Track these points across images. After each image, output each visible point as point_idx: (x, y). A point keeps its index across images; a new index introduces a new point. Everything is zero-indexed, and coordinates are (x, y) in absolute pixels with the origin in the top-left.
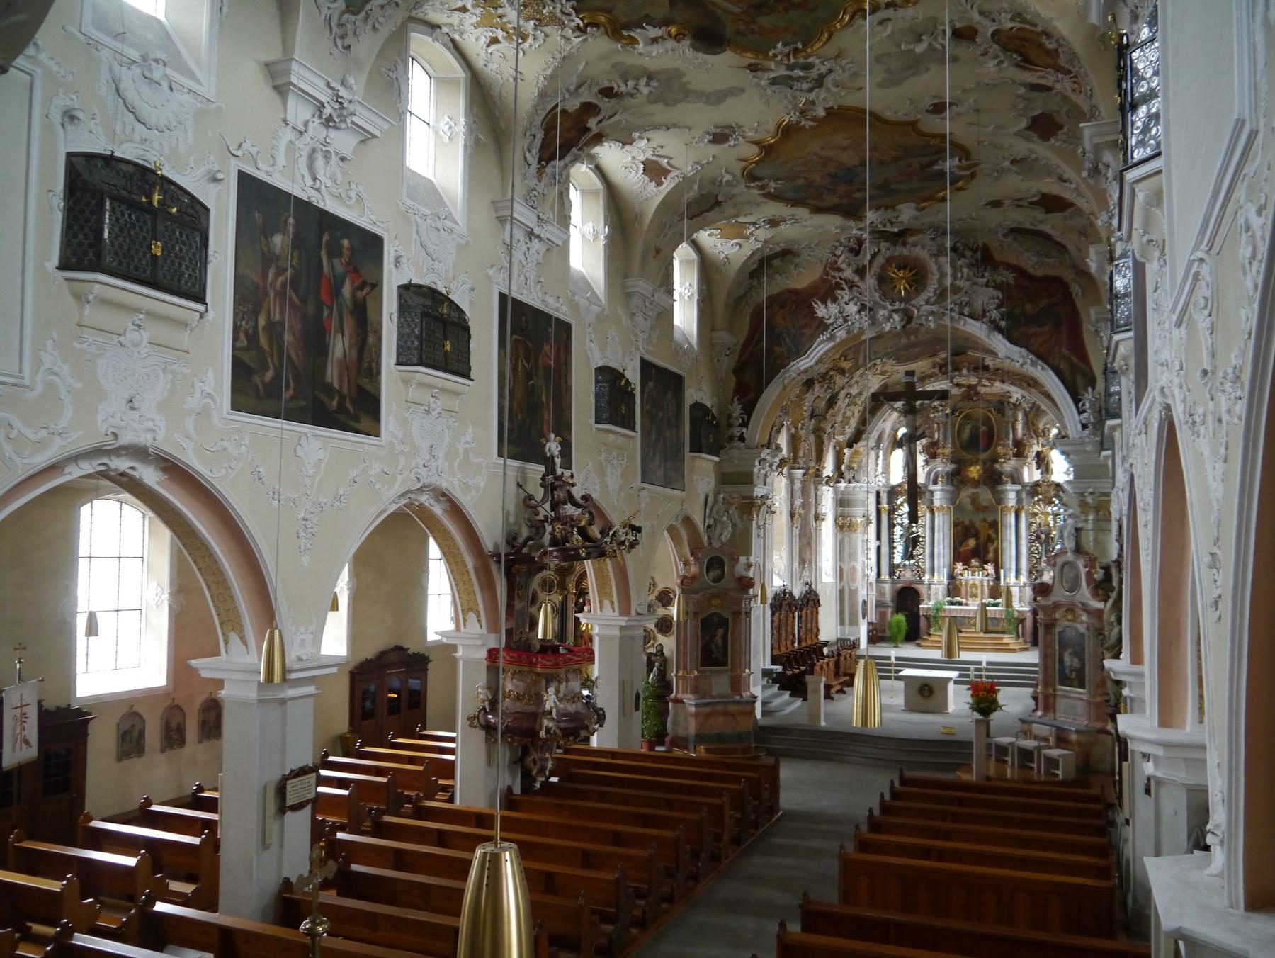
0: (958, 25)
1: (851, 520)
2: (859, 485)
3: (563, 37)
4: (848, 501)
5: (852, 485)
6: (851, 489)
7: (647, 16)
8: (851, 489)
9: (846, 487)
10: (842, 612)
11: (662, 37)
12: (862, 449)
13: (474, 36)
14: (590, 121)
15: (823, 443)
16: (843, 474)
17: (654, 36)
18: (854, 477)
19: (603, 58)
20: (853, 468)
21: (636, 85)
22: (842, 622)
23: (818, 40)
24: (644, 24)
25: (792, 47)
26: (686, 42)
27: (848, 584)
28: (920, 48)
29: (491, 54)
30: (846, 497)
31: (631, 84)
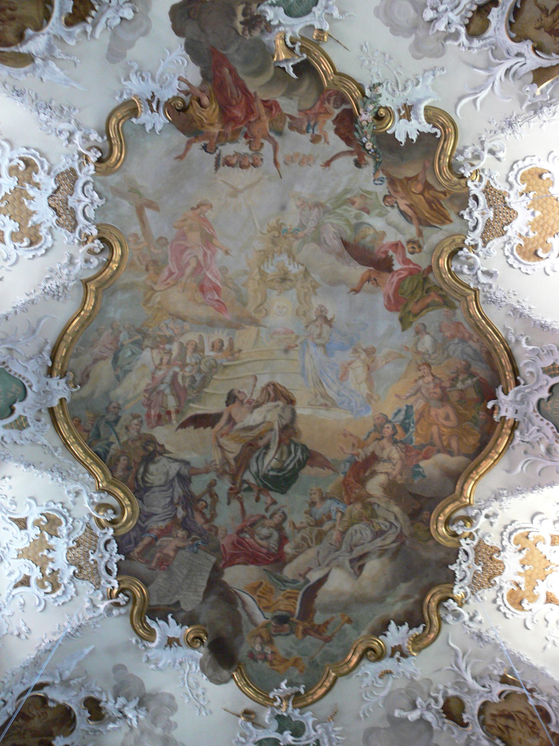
0: (451, 692)
3: (91, 600)
7: (178, 603)
11: (177, 641)
13: (11, 569)
14: (58, 738)
17: (171, 636)
19: (112, 651)
21: (124, 706)
23: (320, 687)
24: (169, 616)
25: (296, 689)
26: (199, 654)
28: (413, 716)
29: (13, 596)
31: (121, 700)
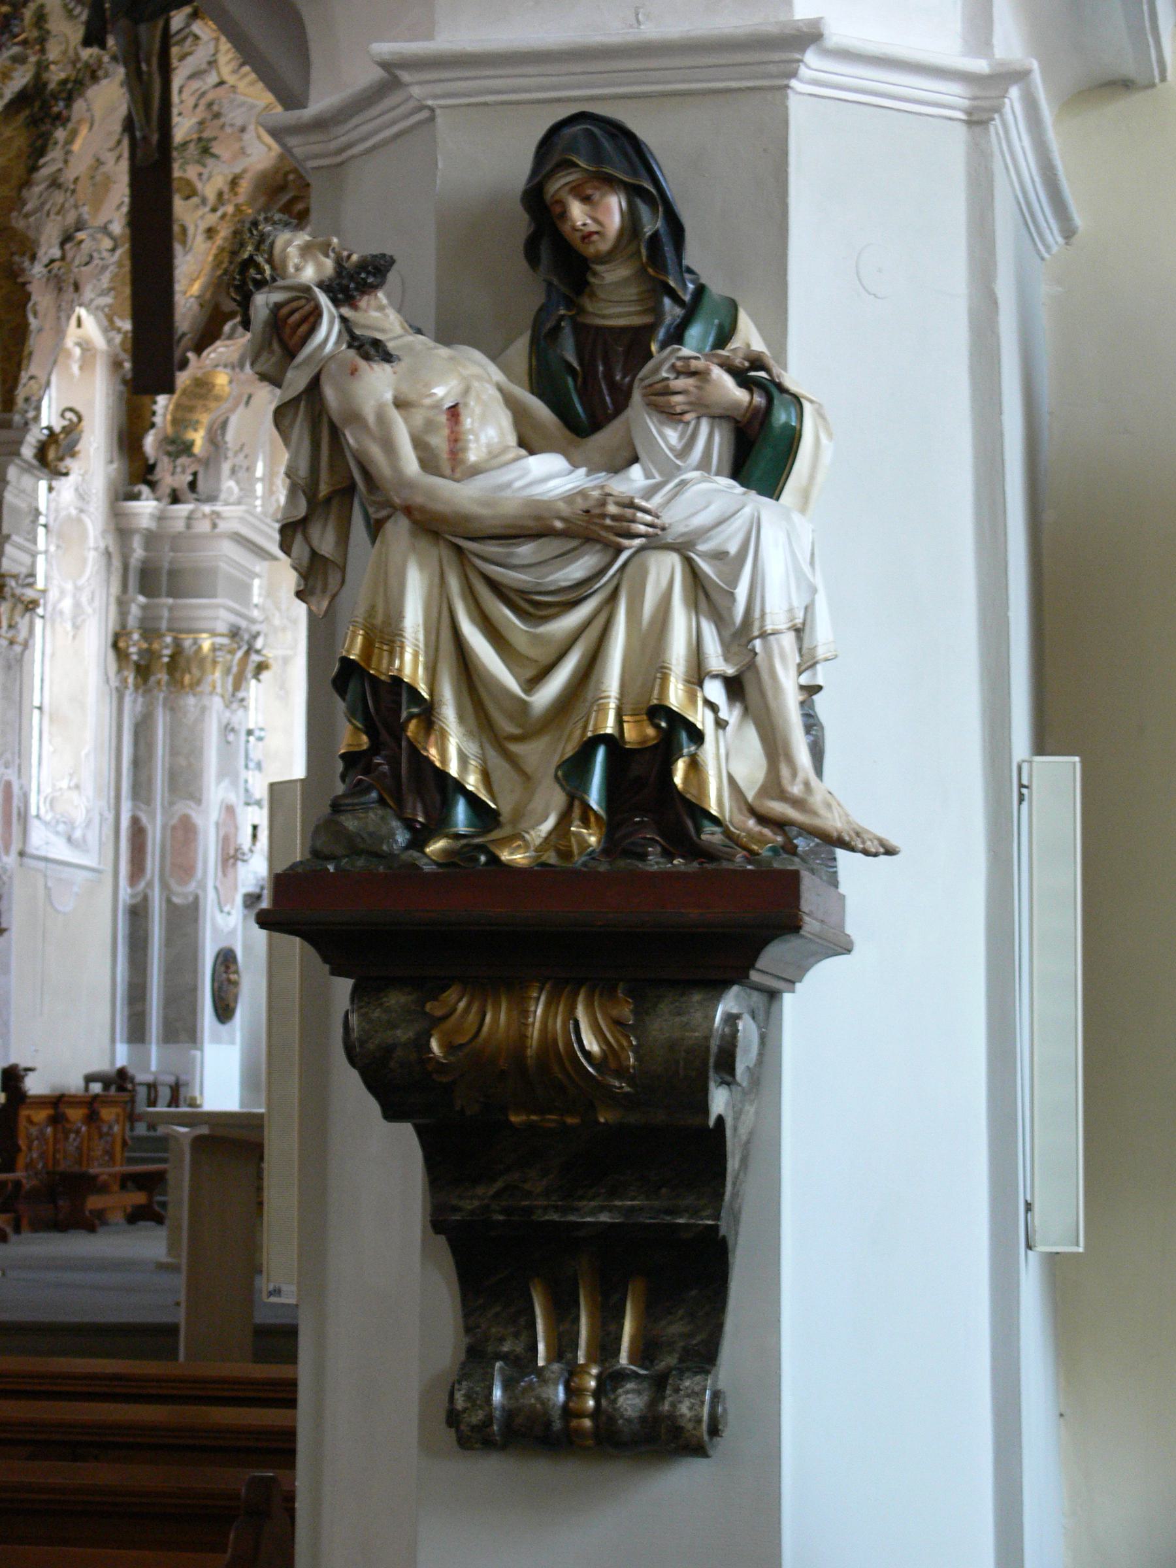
1: (177, 643)
2: (207, 508)
4: (173, 574)
5: (183, 509)
6: (180, 526)
8: (180, 526)
9: (161, 518)
10: (137, 994)
12: (222, 379)
15: (28, 296)
16: (151, 468)
18: (193, 485)
20: (186, 448)
22: (137, 1033)
27: (165, 886)
30: (166, 558)
